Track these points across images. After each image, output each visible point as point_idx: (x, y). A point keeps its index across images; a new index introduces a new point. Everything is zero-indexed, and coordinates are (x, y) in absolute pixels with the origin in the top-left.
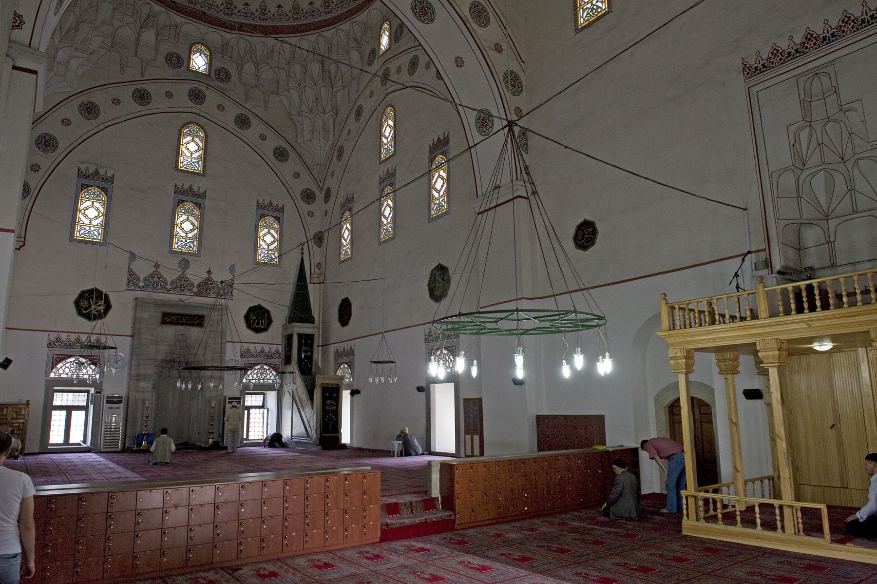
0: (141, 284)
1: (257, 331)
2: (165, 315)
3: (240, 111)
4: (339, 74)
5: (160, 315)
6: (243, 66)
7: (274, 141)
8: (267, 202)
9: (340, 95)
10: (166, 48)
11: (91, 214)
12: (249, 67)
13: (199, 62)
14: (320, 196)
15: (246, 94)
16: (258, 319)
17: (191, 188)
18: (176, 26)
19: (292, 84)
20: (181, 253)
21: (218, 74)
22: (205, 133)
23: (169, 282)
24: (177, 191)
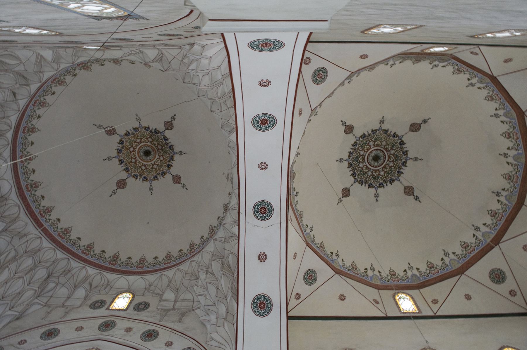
4: (50, 294)
19: (13, 266)
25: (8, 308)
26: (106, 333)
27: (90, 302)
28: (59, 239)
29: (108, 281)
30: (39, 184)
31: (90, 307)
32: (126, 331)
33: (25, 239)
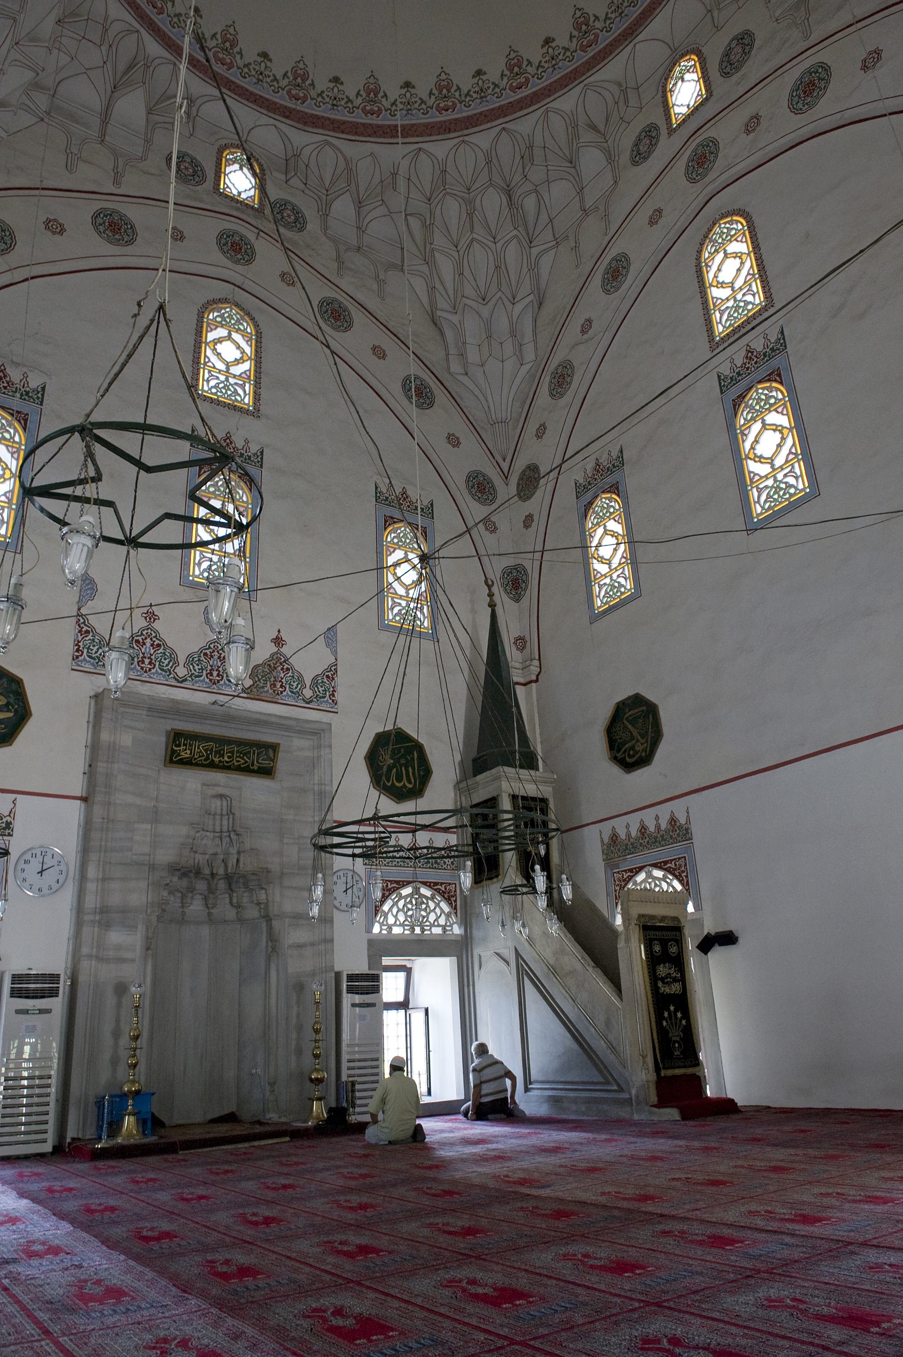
2: (177, 737)
4: (544, 218)
5: (161, 740)
7: (400, 365)
9: (546, 262)
12: (343, 208)
14: (506, 490)
15: (339, 260)
19: (439, 240)
22: (256, 326)
23: (182, 659)
25: (509, 305)
26: (712, 175)
27: (625, 157)
29: (619, 84)
31: (635, 163)
32: (748, 132)
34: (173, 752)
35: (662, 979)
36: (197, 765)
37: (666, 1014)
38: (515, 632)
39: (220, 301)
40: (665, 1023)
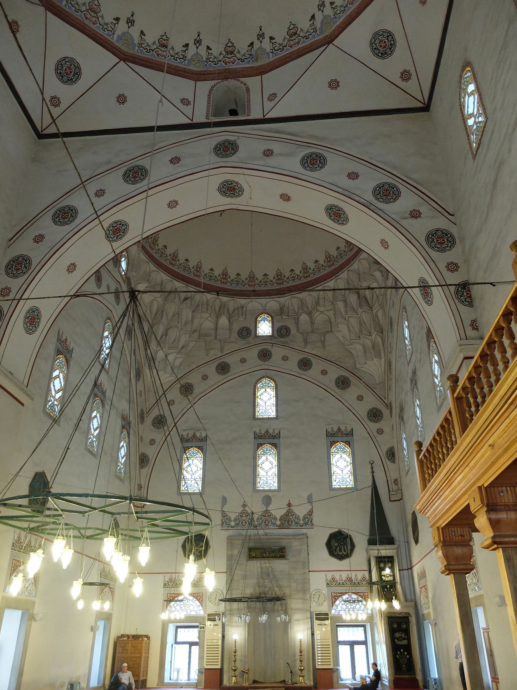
0: (233, 524)
1: (341, 558)
2: (250, 549)
3: (302, 356)
5: (246, 550)
6: (298, 319)
7: (334, 373)
8: (335, 430)
10: (236, 327)
11: (193, 470)
12: (304, 318)
13: (265, 328)
16: (339, 545)
17: (267, 431)
18: (242, 307)
20: (264, 491)
21: (281, 332)
22: (275, 382)
24: (257, 437)
28: (332, 268)
30: (279, 271)
33: (321, 301)
34: (250, 555)
35: (398, 639)
36: (258, 558)
37: (399, 653)
38: (394, 477)
39: (262, 378)
40: (398, 656)
